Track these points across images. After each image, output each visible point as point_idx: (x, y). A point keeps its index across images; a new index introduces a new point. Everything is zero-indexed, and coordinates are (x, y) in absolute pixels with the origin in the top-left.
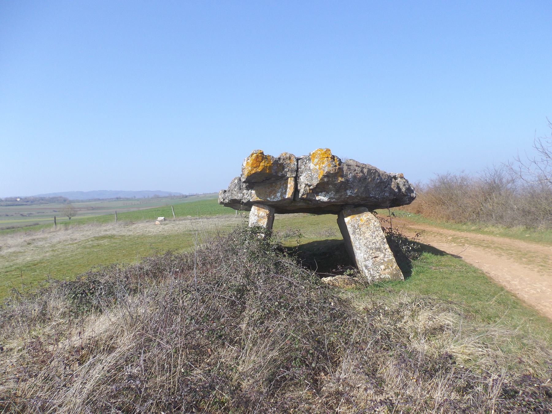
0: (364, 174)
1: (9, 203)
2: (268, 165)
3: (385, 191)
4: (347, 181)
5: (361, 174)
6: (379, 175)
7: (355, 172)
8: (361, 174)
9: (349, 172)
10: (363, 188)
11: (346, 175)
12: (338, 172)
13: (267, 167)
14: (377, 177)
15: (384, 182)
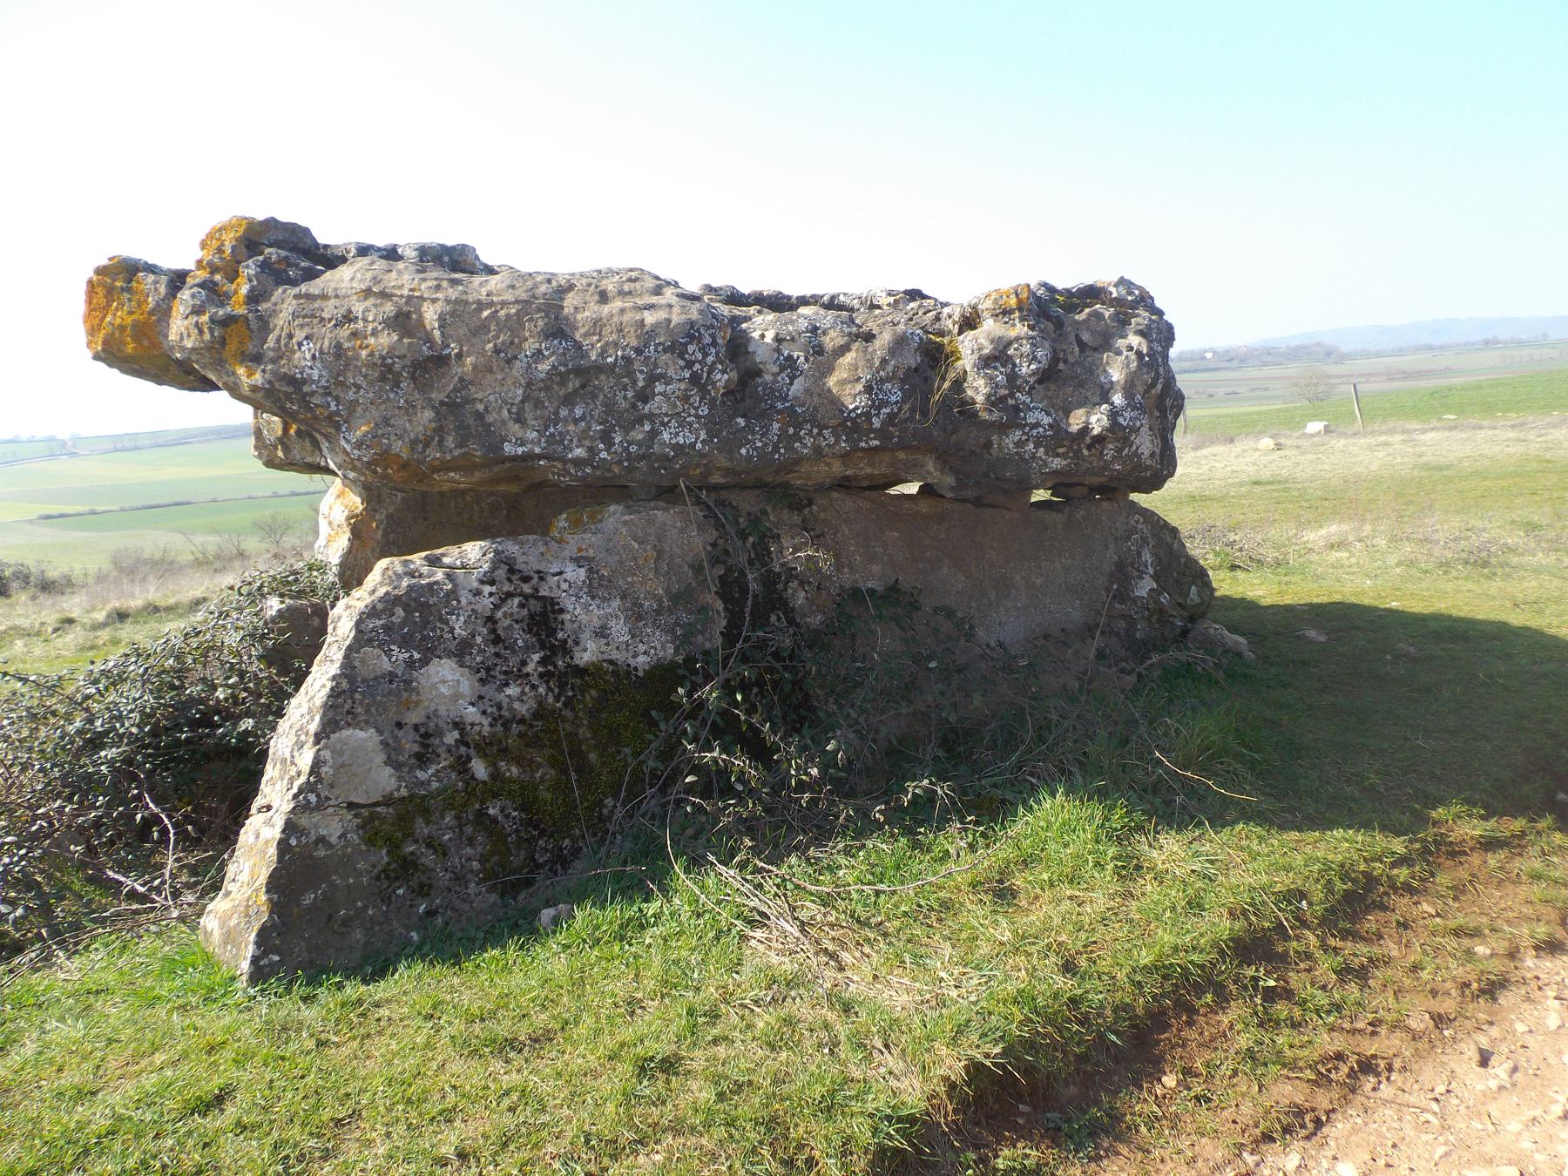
0: (429, 339)
1: (127, 444)
2: (129, 320)
3: (651, 417)
4: (296, 383)
5: (386, 340)
6: (558, 330)
7: (344, 333)
8: (386, 340)
9: (300, 335)
10: (428, 414)
11: (281, 354)
12: (223, 342)
13: (122, 328)
14: (530, 346)
15: (600, 369)
